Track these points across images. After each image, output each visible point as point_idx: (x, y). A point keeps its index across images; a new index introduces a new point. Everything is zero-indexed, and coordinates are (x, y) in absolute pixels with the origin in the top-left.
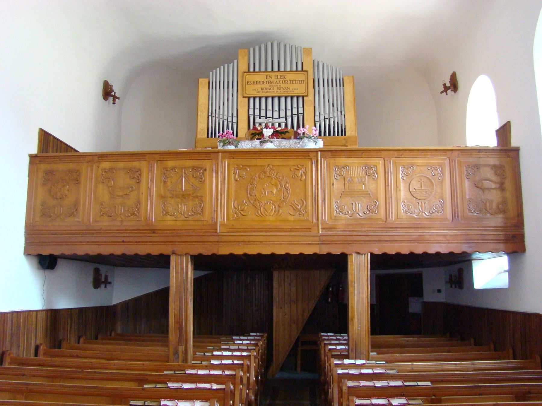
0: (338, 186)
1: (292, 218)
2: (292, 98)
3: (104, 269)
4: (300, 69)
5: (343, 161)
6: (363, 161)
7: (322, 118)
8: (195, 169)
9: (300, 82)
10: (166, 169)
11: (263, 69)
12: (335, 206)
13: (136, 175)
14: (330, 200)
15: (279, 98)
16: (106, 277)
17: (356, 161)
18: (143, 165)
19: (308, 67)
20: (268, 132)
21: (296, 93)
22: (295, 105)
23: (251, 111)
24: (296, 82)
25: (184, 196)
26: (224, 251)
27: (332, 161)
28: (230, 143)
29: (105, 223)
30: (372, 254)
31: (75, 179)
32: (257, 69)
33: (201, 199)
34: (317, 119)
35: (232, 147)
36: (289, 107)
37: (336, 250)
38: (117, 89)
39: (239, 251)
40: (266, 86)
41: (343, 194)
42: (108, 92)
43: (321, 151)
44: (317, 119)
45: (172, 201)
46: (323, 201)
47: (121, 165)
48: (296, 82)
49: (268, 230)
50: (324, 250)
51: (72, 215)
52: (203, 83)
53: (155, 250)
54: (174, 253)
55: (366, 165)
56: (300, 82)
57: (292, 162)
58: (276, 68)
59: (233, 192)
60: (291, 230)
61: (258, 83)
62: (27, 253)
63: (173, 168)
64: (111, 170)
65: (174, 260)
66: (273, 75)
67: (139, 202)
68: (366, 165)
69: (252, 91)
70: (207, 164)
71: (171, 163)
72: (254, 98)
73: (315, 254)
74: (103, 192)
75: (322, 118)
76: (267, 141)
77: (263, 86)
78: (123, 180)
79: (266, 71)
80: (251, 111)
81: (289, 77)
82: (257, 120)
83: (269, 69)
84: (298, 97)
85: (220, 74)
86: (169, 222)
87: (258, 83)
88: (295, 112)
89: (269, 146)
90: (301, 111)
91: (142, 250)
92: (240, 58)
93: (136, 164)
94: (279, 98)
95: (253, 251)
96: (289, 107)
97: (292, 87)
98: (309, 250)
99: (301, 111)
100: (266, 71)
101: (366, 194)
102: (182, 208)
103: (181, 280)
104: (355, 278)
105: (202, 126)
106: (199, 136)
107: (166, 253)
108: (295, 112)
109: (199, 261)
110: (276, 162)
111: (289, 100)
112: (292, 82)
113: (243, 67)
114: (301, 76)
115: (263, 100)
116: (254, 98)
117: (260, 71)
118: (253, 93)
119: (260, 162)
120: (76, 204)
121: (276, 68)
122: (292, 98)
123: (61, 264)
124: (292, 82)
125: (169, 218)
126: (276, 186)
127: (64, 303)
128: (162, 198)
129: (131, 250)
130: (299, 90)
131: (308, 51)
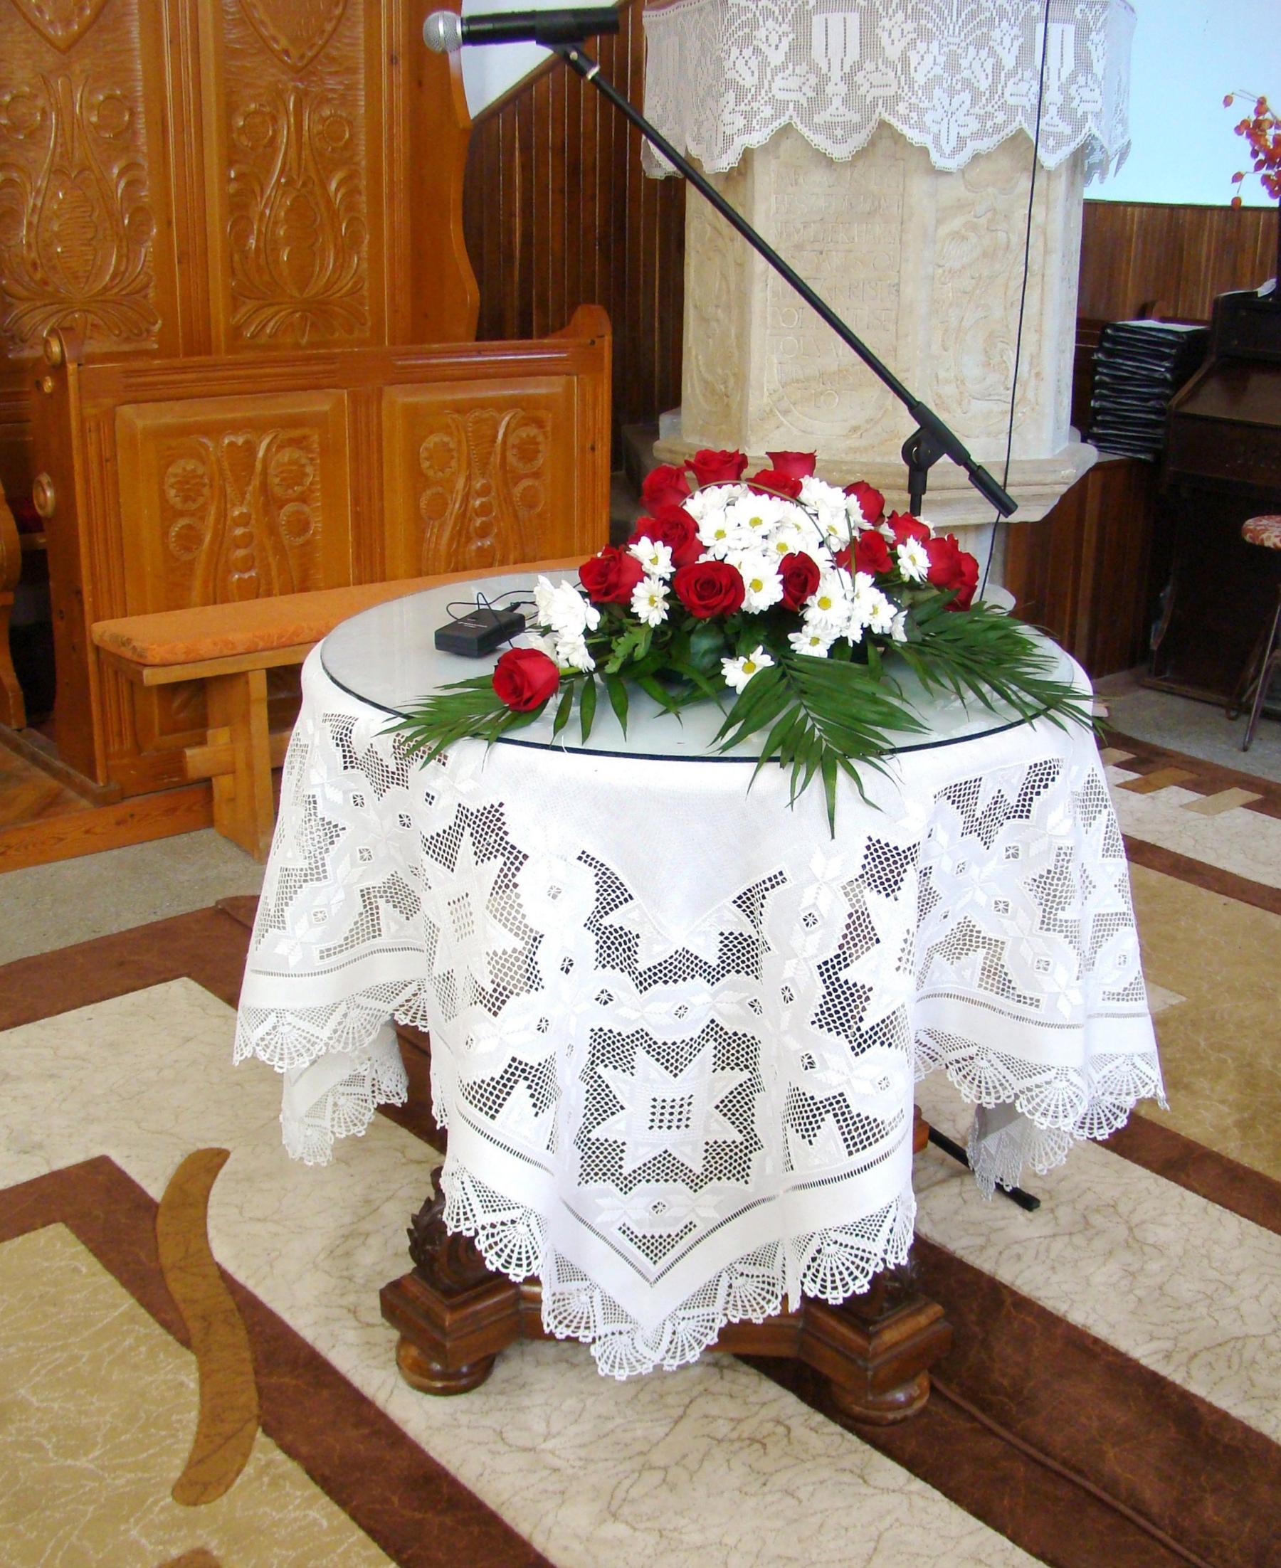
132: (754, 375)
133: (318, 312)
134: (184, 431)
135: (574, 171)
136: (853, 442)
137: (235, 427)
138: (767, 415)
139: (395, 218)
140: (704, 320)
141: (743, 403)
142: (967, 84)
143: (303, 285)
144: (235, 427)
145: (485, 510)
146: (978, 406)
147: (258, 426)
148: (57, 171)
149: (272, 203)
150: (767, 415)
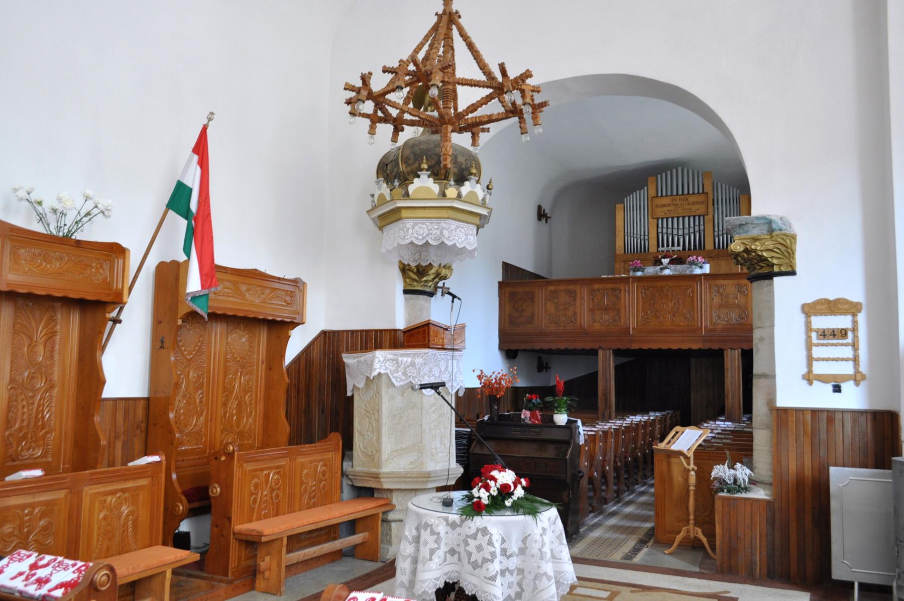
0: (717, 300)
1: (682, 324)
2: (694, 217)
3: (544, 357)
4: (701, 191)
5: (722, 282)
6: (735, 282)
7: (720, 233)
8: (613, 290)
9: (702, 203)
10: (593, 290)
11: (669, 194)
12: (714, 315)
13: (572, 295)
14: (711, 312)
15: (684, 218)
16: (547, 363)
17: (731, 282)
18: (577, 288)
19: (708, 189)
20: (665, 261)
21: (698, 212)
22: (697, 223)
23: (660, 230)
24: (697, 203)
25: (606, 309)
26: (635, 347)
27: (712, 282)
28: (638, 270)
29: (552, 328)
30: (742, 350)
31: (531, 298)
32: (664, 194)
33: (618, 311)
34: (716, 234)
35: (639, 274)
36: (692, 225)
37: (715, 347)
38: (547, 209)
39: (645, 347)
40: (672, 208)
41: (721, 306)
42: (541, 215)
43: (705, 275)
44: (716, 234)
45: (598, 313)
46: (706, 311)
47: (562, 288)
48: (697, 203)
49: (666, 332)
50: (707, 346)
51: (530, 322)
52: (619, 207)
53: (588, 346)
54: (600, 348)
55: (738, 285)
56: (702, 203)
57: (682, 283)
58: (680, 192)
59: (640, 307)
60: (682, 332)
61: (665, 206)
62: (500, 348)
63: (598, 290)
64: (555, 291)
65: (600, 353)
66: (677, 198)
67: (575, 313)
68: (738, 285)
69: (660, 212)
70: (622, 286)
71: (596, 286)
72: (662, 219)
73: (700, 350)
74: (551, 307)
75: (720, 233)
76: (666, 268)
77: (669, 208)
78: (563, 298)
79: (672, 195)
80: (660, 230)
81: (691, 199)
82: (660, 249)
83: (675, 193)
84: (699, 216)
85: (632, 200)
86: (597, 326)
87: (665, 206)
88: (697, 228)
89: (667, 272)
90: (702, 227)
91: (579, 346)
92: (649, 185)
93: (571, 287)
94: (684, 218)
95: (655, 346)
96: (692, 225)
97: (694, 207)
98: (695, 347)
99: (702, 227)
100: (672, 195)
101: (738, 306)
102: (606, 317)
103: (606, 367)
104: (729, 367)
105: (619, 243)
106: (618, 252)
107: (595, 348)
108: (697, 228)
109: (618, 353)
110: (671, 283)
111: (692, 218)
112: (694, 203)
113: (652, 193)
114: (702, 198)
115: (670, 220)
116: (662, 219)
117: (666, 195)
118: (662, 215)
119: (659, 284)
120: (533, 315)
121: (680, 192)
122: (694, 217)
123: (519, 354)
124: (694, 203)
125: (596, 324)
126: (671, 301)
127: (520, 383)
128: (592, 311)
129: (571, 346)
130: (701, 209)
131: (707, 174)
132: (383, 449)
133: (241, 434)
134: (256, 470)
135: (298, 391)
136: (411, 466)
137: (266, 469)
138: (387, 460)
139: (261, 406)
140: (361, 434)
141: (380, 457)
142: (434, 375)
143: (238, 427)
144: (266, 469)
145: (315, 491)
146: (440, 455)
147: (271, 468)
148: (184, 396)
149: (233, 404)
150: (387, 460)
